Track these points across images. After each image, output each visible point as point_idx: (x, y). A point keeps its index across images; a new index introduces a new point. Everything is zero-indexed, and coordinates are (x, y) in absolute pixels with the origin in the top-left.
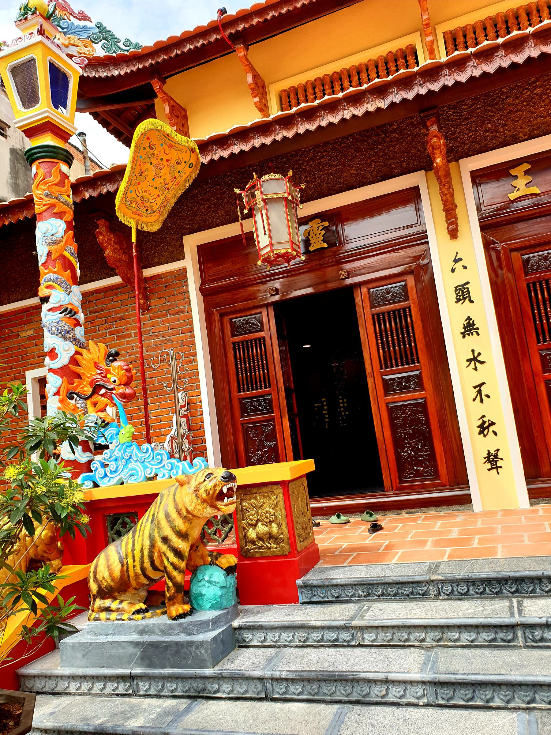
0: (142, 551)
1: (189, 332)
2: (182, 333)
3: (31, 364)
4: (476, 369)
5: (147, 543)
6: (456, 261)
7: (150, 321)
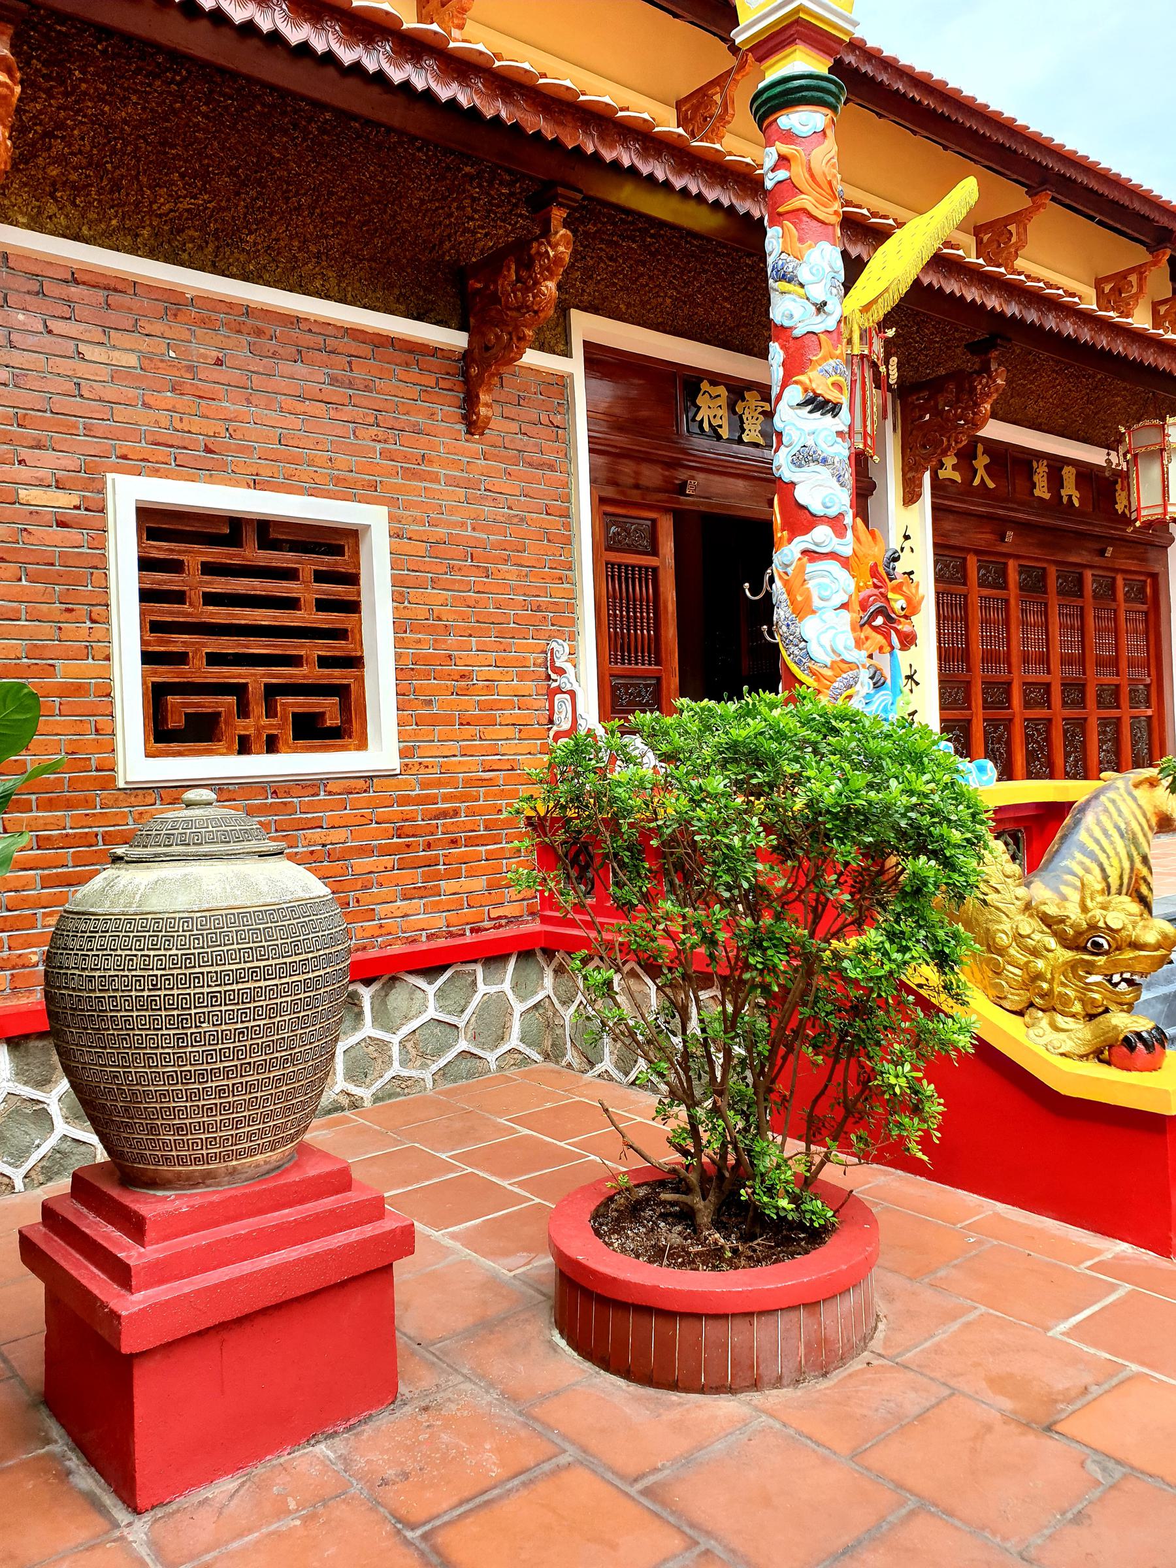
0: (1121, 877)
1: (560, 516)
2: (547, 514)
3: (124, 457)
4: (911, 691)
5: (1127, 865)
6: (907, 537)
7: (483, 462)
